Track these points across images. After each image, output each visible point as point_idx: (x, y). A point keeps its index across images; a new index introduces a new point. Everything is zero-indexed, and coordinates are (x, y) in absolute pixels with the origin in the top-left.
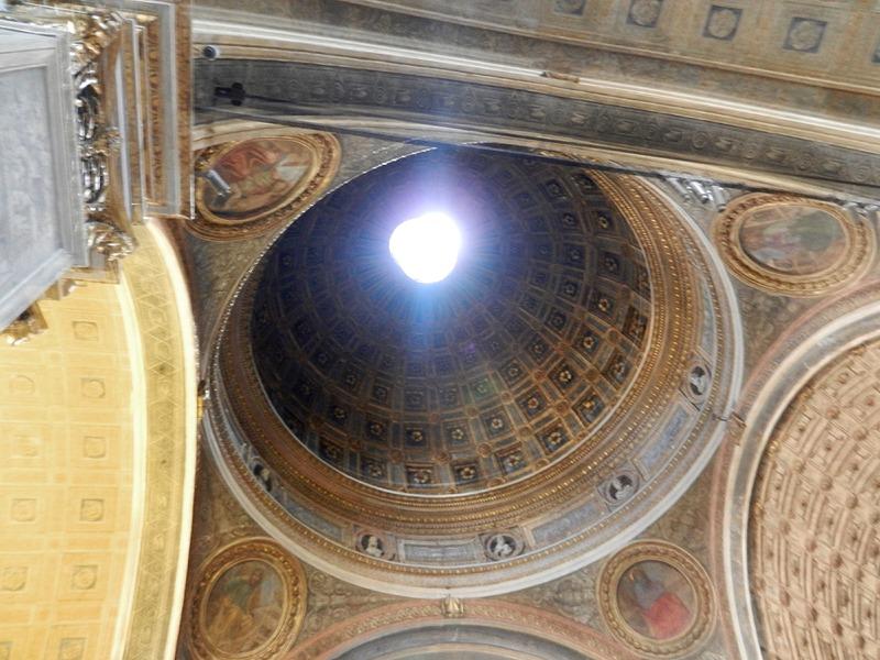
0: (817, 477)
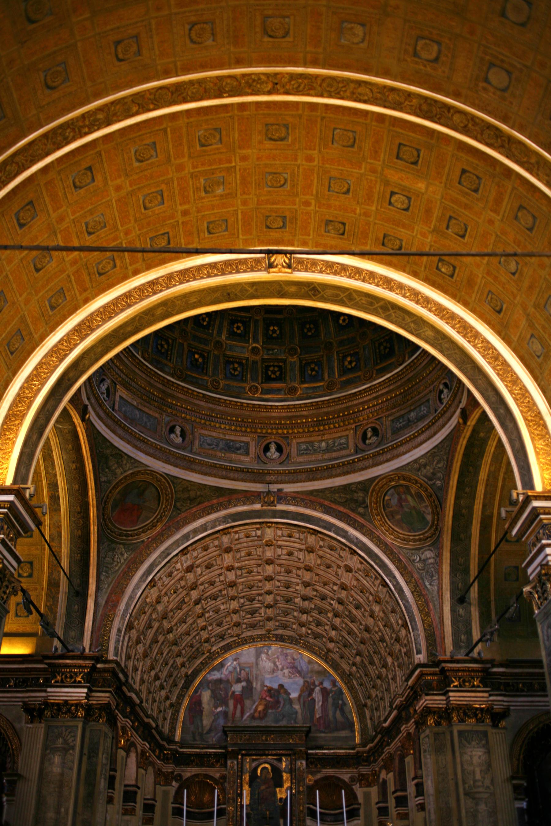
0: (269, 554)
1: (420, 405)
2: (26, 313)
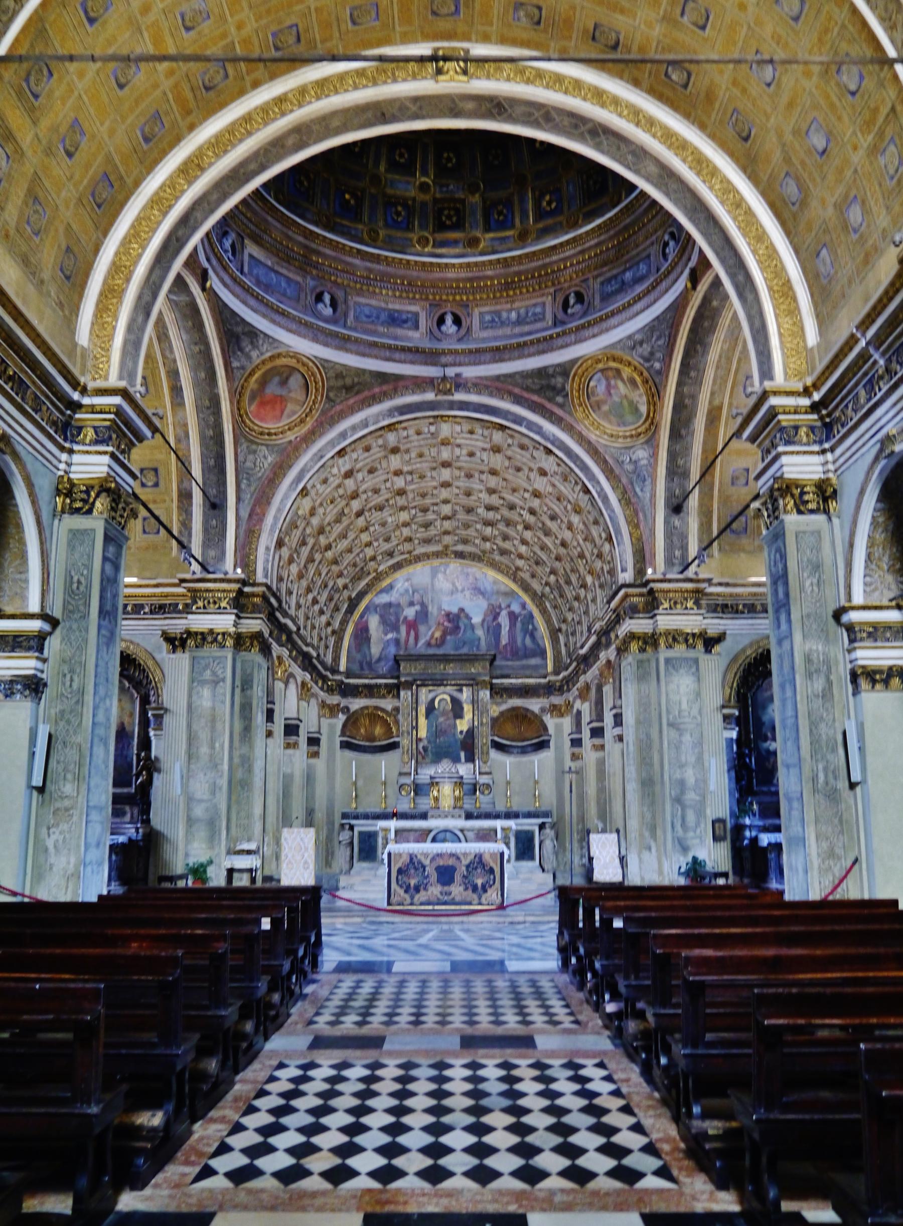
0: (445, 454)
1: (638, 263)
2: (112, 149)
